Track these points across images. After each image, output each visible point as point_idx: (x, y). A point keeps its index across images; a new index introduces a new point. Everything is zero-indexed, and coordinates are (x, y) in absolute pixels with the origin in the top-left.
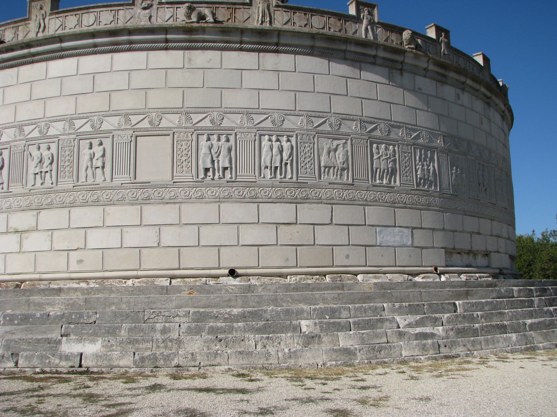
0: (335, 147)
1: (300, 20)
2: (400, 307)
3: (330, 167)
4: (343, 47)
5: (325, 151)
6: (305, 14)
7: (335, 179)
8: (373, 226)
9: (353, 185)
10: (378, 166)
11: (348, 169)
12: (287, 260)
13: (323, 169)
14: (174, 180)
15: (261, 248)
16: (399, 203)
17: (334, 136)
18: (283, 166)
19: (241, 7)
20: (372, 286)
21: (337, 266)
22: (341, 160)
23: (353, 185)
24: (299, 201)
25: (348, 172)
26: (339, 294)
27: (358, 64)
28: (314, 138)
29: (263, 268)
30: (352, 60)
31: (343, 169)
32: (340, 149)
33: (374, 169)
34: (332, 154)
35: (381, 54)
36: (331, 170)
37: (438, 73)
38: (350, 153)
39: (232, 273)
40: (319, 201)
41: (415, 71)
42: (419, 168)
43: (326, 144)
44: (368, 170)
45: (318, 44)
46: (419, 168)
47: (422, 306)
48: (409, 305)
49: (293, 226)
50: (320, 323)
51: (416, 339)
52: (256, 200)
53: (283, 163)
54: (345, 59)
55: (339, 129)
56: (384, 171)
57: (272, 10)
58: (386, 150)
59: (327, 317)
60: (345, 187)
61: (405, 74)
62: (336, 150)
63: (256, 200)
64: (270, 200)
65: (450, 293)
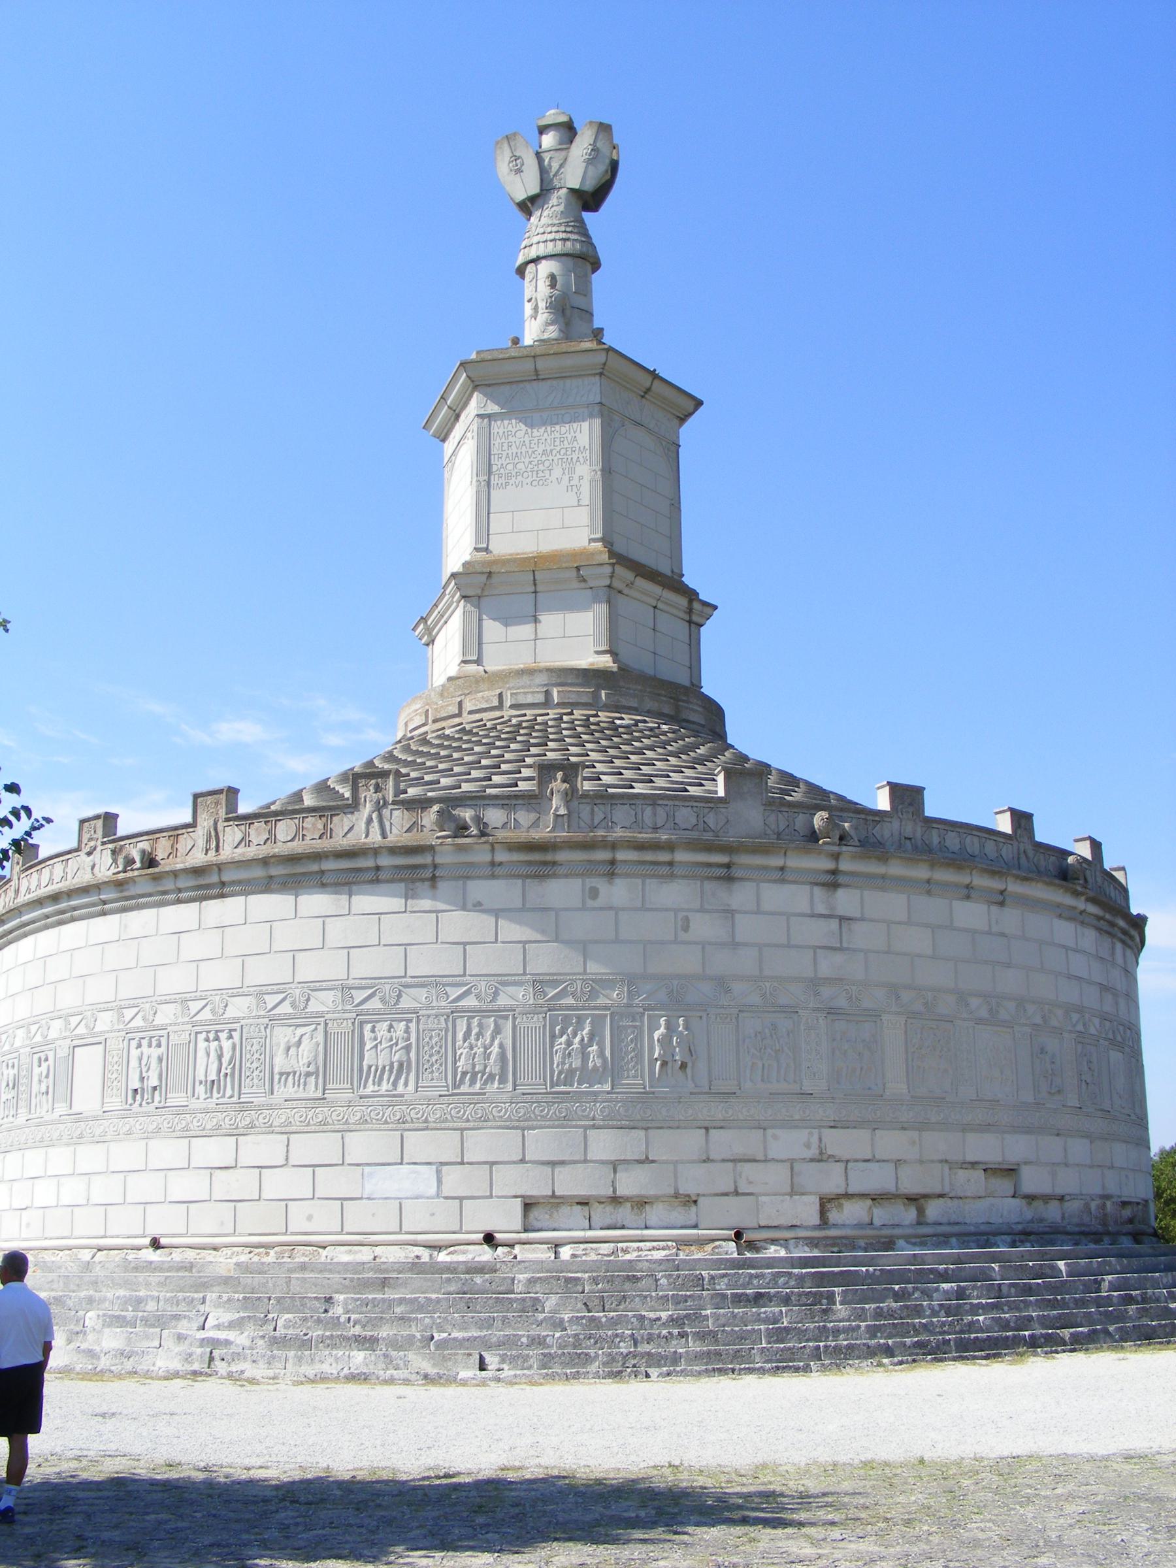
0: (297, 1039)
1: (259, 834)
2: (229, 1300)
3: (288, 1074)
4: (315, 867)
5: (283, 1046)
6: (266, 822)
7: (296, 1092)
8: (358, 1165)
9: (325, 1099)
10: (373, 1062)
11: (317, 1073)
12: (222, 1223)
13: (277, 1077)
14: (105, 1109)
15: (192, 1206)
16: (412, 1122)
17: (300, 1018)
18: (222, 1078)
19: (184, 831)
20: (232, 1266)
21: (292, 1234)
22: (306, 1061)
23: (325, 1099)
24: (241, 1131)
25: (317, 1078)
26: (167, 1278)
27: (346, 888)
28: (265, 1028)
29: (193, 1236)
30: (337, 884)
31: (308, 1074)
32: (305, 1040)
33: (365, 1068)
34: (293, 1051)
35: (385, 861)
36: (291, 1077)
37: (529, 863)
38: (321, 1048)
39: (156, 1244)
40: (269, 1130)
41: (466, 873)
42: (461, 1054)
43: (283, 1035)
44: (352, 1070)
45: (275, 871)
46: (461, 1054)
47: (266, 1300)
48: (245, 1298)
49: (232, 1170)
50: (104, 1315)
51: (201, 1346)
52: (188, 1134)
53: (222, 1074)
54: (323, 885)
55: (306, 1007)
56: (384, 1067)
57: (220, 827)
58: (389, 1031)
59: (130, 1309)
60: (309, 1104)
61: (441, 885)
62: (299, 1043)
63: (188, 1134)
64: (204, 1133)
65: (347, 1282)
